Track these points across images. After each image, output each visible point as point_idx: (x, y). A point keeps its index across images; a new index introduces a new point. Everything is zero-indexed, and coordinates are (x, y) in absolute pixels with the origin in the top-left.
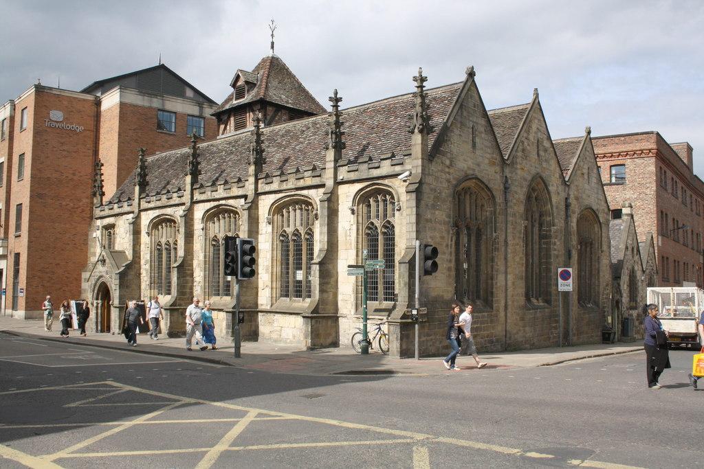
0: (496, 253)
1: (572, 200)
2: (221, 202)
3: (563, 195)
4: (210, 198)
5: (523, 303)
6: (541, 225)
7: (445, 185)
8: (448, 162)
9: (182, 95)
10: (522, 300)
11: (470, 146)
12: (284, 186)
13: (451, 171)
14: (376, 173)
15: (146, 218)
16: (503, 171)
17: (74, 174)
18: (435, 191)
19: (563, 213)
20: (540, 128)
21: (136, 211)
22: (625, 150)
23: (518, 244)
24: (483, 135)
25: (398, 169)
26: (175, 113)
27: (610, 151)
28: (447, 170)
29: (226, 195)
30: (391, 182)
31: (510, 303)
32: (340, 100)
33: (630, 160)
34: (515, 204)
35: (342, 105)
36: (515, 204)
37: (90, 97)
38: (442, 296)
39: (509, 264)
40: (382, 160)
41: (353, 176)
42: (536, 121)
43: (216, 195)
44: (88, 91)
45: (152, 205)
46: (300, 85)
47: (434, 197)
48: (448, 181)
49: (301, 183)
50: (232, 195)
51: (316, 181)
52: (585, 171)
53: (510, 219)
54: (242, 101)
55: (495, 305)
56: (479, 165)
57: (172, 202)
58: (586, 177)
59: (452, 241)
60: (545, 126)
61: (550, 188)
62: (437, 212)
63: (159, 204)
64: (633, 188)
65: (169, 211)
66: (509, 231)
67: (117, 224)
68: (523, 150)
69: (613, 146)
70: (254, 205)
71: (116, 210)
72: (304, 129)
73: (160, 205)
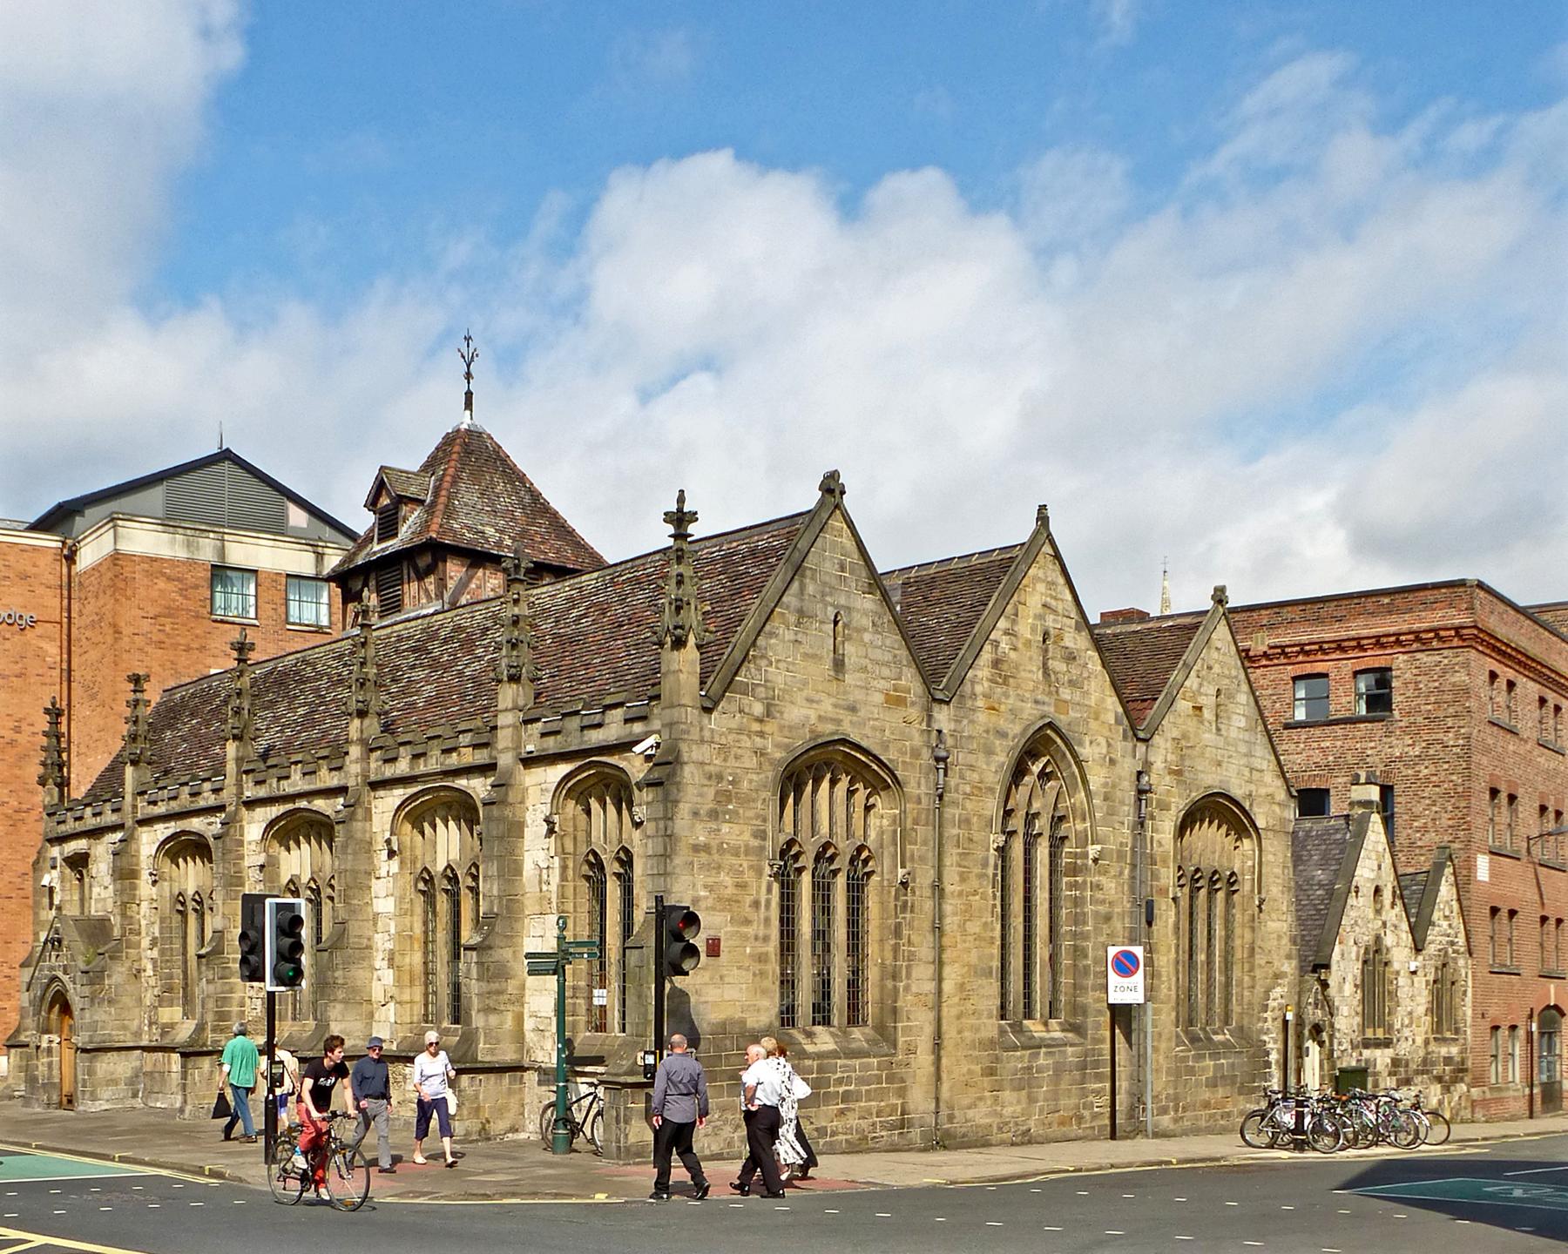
0: (908, 915)
1: (1159, 780)
2: (303, 804)
3: (1128, 767)
4: (276, 793)
5: (995, 1033)
6: (1057, 843)
7: (750, 762)
8: (758, 709)
9: (276, 528)
10: (990, 1027)
11: (828, 664)
12: (422, 768)
13: (768, 728)
14: (595, 737)
15: (149, 841)
16: (930, 717)
17: (17, 730)
18: (720, 778)
19: (1127, 813)
20: (1053, 603)
21: (129, 823)
22: (1392, 630)
23: (975, 893)
24: (867, 637)
25: (638, 728)
26: (255, 571)
27: (1353, 633)
28: (756, 727)
29: (307, 788)
30: (625, 759)
32: (693, 517)
33: (1406, 657)
34: (967, 796)
35: (696, 530)
36: (967, 796)
37: (50, 541)
38: (743, 1022)
39: (946, 941)
40: (564, 715)
41: (551, 745)
42: (1041, 587)
43: (287, 787)
44: (47, 523)
45: (161, 809)
46: (535, 496)
47: (717, 793)
48: (760, 753)
49: (453, 760)
50: (319, 785)
51: (481, 757)
52: (1208, 701)
53: (952, 831)
54: (393, 545)
55: (901, 1040)
56: (853, 709)
57: (202, 803)
58: (1208, 714)
59: (769, 890)
60: (1069, 597)
61: (1085, 751)
62: (725, 828)
63: (175, 806)
64: (1412, 730)
65: (196, 824)
66: (947, 861)
67: (92, 852)
68: (996, 663)
69: (1360, 622)
70: (360, 812)
71: (91, 822)
72: (489, 624)
73: (177, 809)
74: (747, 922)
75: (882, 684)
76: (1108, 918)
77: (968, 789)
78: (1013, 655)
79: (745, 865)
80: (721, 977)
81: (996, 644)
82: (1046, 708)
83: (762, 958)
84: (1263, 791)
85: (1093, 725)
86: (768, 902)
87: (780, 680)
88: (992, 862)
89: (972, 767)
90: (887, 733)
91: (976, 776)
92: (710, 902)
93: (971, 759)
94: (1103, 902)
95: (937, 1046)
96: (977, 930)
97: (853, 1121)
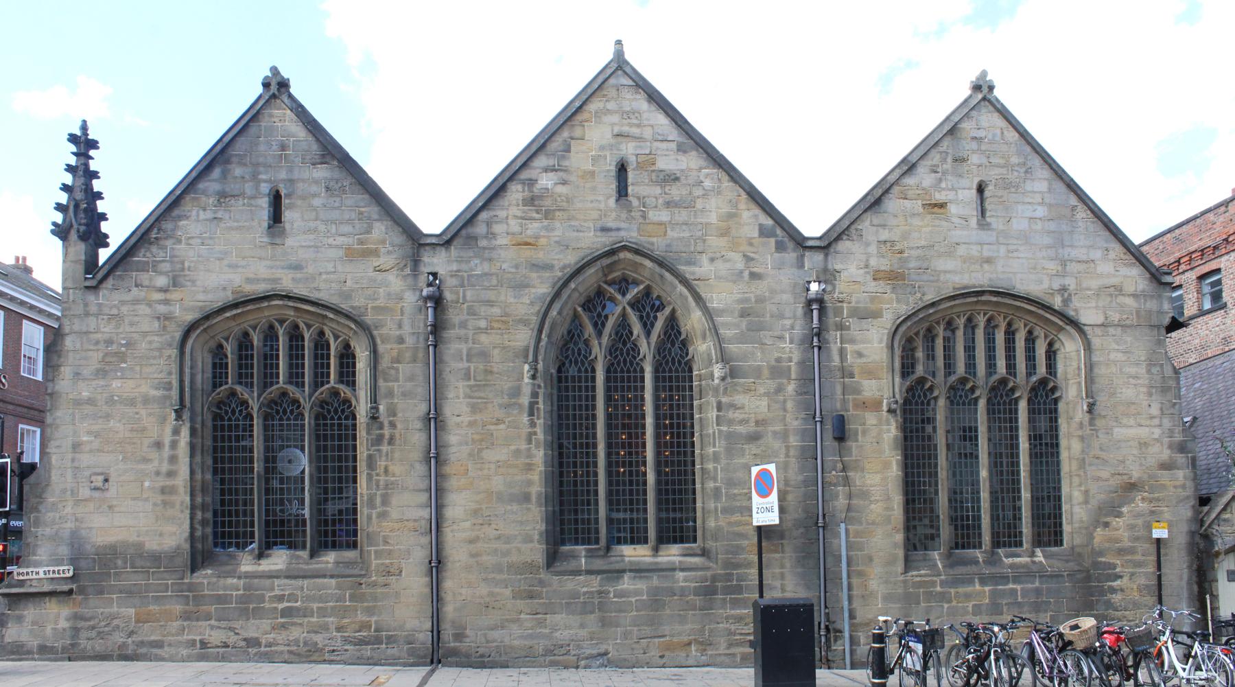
13: (175, 295)
23: (499, 421)
24: (317, 202)
31: (457, 554)
39: (447, 469)
62: (116, 384)
68: (531, 201)
74: (146, 460)
75: (340, 240)
76: (754, 438)
77: (483, 324)
78: (561, 189)
79: (143, 412)
80: (110, 507)
81: (531, 182)
82: (623, 234)
83: (171, 490)
84: (1095, 284)
85: (715, 242)
86: (174, 445)
87: (191, 253)
88: (527, 390)
89: (490, 303)
90: (349, 283)
91: (496, 311)
92: (96, 445)
93: (491, 295)
94: (743, 422)
95: (437, 565)
96: (503, 458)
97: (296, 633)
